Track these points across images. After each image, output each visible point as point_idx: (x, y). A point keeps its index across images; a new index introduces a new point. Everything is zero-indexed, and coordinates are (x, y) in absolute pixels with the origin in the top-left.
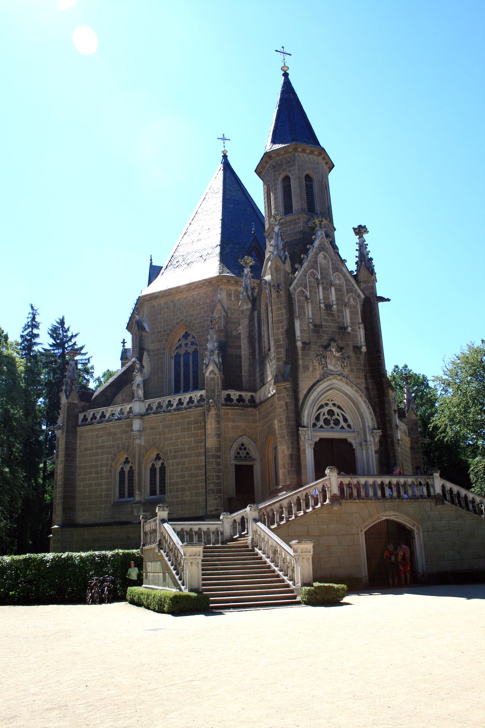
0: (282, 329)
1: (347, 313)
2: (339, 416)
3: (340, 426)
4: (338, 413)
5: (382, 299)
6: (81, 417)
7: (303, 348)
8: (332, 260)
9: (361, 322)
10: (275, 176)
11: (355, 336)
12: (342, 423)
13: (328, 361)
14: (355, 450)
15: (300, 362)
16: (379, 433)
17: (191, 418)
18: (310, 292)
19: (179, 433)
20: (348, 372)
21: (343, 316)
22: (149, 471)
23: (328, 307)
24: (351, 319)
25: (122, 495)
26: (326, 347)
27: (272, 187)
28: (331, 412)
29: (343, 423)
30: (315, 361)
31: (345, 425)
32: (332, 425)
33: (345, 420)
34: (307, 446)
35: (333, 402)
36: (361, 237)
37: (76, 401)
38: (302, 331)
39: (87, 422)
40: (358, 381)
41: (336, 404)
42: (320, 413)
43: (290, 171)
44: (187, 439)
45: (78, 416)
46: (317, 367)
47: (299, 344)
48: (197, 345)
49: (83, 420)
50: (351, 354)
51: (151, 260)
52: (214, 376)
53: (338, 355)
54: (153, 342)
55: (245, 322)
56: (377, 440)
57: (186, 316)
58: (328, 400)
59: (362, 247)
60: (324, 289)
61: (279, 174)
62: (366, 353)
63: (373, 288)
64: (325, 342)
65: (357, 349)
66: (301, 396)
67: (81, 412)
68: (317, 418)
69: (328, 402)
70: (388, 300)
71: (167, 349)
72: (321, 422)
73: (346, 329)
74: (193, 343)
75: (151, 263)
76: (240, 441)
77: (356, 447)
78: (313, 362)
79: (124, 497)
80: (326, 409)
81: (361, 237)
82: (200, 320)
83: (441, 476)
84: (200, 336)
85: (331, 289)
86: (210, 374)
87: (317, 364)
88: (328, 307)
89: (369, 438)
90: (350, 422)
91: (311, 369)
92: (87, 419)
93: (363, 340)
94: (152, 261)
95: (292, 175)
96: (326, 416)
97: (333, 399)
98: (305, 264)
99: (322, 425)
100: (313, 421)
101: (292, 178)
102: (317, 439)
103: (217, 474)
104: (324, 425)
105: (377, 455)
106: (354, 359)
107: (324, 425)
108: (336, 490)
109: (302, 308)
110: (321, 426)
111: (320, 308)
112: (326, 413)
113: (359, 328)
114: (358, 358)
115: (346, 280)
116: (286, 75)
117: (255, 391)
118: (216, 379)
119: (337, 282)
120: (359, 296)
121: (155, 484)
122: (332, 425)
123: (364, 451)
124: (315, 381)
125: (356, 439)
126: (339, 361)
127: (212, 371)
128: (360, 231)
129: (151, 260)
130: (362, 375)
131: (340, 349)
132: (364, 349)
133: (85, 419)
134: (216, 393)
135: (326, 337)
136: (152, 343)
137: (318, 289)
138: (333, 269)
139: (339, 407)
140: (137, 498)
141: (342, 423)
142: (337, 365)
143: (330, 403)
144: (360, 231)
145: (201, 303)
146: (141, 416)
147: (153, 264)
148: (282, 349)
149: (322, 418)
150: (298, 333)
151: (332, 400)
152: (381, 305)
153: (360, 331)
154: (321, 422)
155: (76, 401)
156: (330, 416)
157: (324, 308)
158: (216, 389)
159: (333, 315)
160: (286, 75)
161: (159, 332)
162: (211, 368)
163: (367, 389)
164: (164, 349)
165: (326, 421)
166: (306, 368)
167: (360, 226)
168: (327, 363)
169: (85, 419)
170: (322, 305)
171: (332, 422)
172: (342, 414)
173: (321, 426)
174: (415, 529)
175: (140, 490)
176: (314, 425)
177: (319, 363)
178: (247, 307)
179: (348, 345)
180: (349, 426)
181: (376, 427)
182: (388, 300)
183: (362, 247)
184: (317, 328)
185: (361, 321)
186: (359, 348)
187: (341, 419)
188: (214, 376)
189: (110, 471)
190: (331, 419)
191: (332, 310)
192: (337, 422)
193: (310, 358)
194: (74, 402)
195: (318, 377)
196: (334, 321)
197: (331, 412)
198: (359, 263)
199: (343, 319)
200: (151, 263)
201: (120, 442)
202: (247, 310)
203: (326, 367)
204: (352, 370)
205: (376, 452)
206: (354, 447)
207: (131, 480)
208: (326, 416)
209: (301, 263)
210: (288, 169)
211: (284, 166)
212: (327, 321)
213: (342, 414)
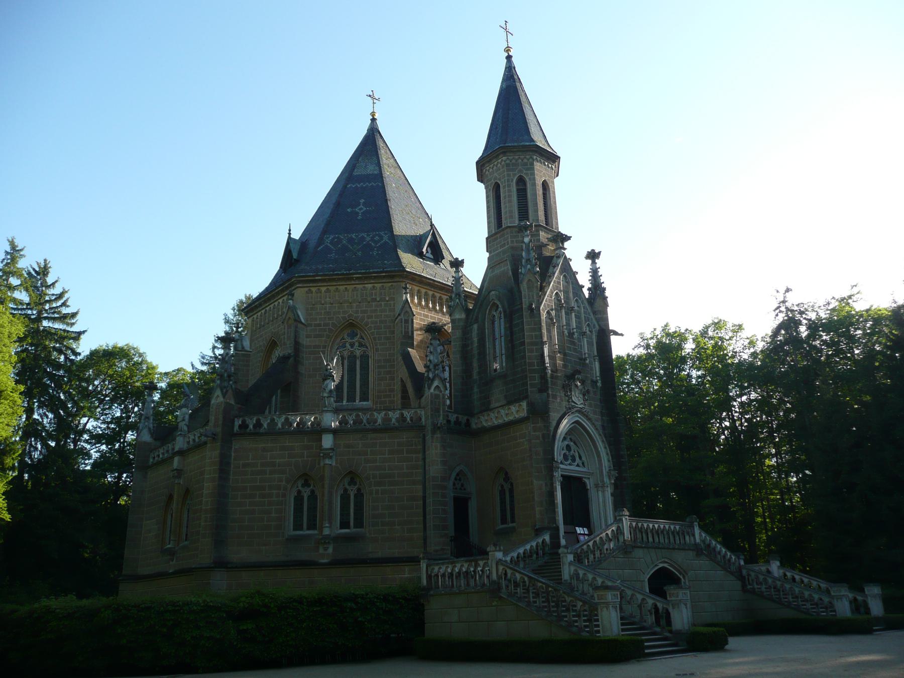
0: (536, 352)
3: (576, 464)
5: (616, 333)
6: (238, 422)
8: (572, 284)
9: (596, 354)
10: (509, 175)
11: (592, 369)
13: (573, 393)
14: (589, 493)
17: (403, 438)
19: (385, 455)
21: (581, 345)
22: (339, 498)
23: (571, 334)
24: (588, 351)
25: (298, 526)
27: (504, 187)
32: (569, 461)
33: (580, 458)
34: (557, 483)
36: (594, 263)
37: (232, 402)
39: (248, 430)
40: (596, 416)
43: (527, 174)
44: (396, 464)
45: (233, 422)
46: (564, 398)
48: (367, 347)
49: (240, 426)
50: (590, 389)
51: (290, 230)
52: (438, 393)
54: (307, 337)
55: (457, 333)
56: (613, 481)
57: (357, 312)
59: (595, 274)
60: (567, 314)
61: (514, 175)
62: (601, 387)
63: (606, 320)
65: (594, 383)
66: (552, 429)
67: (238, 416)
70: (622, 335)
71: (328, 348)
73: (585, 359)
74: (361, 345)
75: (290, 234)
76: (457, 470)
77: (591, 488)
78: (560, 392)
79: (301, 529)
80: (566, 443)
81: (594, 263)
82: (376, 320)
83: (700, 527)
84: (375, 339)
85: (571, 314)
86: (434, 390)
87: (563, 395)
89: (606, 480)
92: (247, 426)
93: (598, 374)
94: (291, 232)
95: (530, 179)
96: (565, 451)
101: (529, 183)
103: (443, 507)
104: (563, 461)
105: (613, 498)
106: (592, 394)
107: (563, 461)
111: (563, 334)
112: (565, 448)
113: (594, 360)
116: (509, 58)
117: (472, 415)
118: (441, 396)
121: (349, 514)
122: (569, 461)
123: (600, 493)
124: (562, 413)
125: (591, 479)
127: (437, 387)
128: (593, 256)
129: (290, 230)
132: (599, 384)
133: (244, 426)
134: (441, 413)
136: (307, 337)
137: (561, 313)
138: (573, 293)
139: (575, 443)
140: (326, 532)
142: (579, 398)
143: (569, 439)
144: (593, 256)
145: (378, 299)
146: (334, 432)
147: (292, 236)
148: (537, 375)
152: (613, 338)
153: (595, 364)
155: (232, 402)
157: (567, 334)
158: (441, 408)
159: (573, 343)
160: (509, 58)
161: (319, 325)
163: (603, 426)
164: (325, 347)
167: (593, 250)
168: (571, 394)
169: (244, 426)
170: (566, 332)
171: (570, 458)
174: (681, 577)
175: (330, 523)
177: (565, 394)
178: (460, 317)
180: (583, 464)
181: (612, 468)
182: (622, 335)
183: (595, 274)
185: (596, 354)
186: (596, 382)
187: (577, 455)
188: (438, 393)
189: (284, 496)
191: (573, 338)
192: (574, 460)
194: (231, 402)
196: (575, 350)
198: (593, 290)
199: (582, 349)
200: (290, 234)
201: (300, 460)
202: (460, 320)
203: (571, 397)
204: (590, 405)
205: (612, 495)
206: (589, 488)
207: (313, 509)
210: (524, 171)
211: (520, 167)
212: (570, 349)
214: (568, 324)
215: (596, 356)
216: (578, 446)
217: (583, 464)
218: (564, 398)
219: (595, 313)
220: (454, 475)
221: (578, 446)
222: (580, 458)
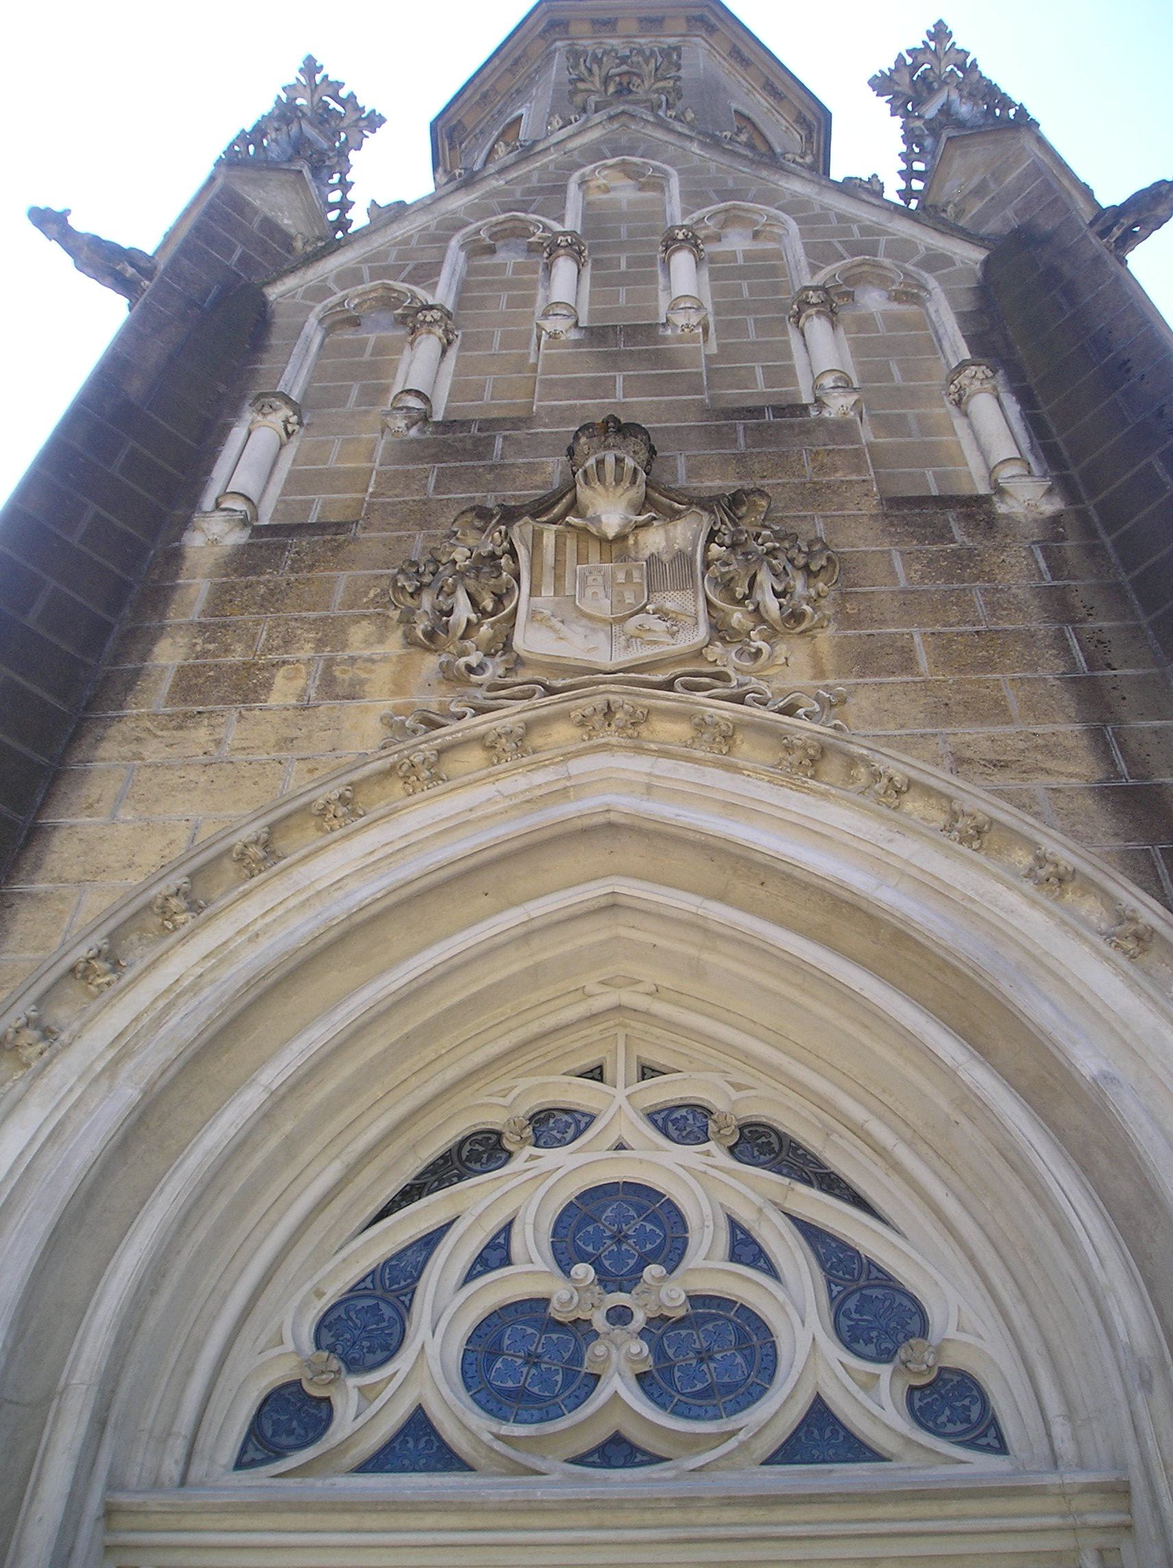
2: (771, 1270)
4: (746, 1217)
20: (820, 673)
29: (833, 1351)
30: (358, 634)
35: (662, 1092)
41: (718, 1103)
42: (430, 1241)
58: (596, 1073)
69: (582, 1095)
85: (666, 264)
97: (657, 1058)
99: (437, 1413)
110: (419, 1423)
126: (686, 581)
151: (647, 1072)
156: (583, 1271)
172: (811, 1233)
173: (419, 1423)
190: (620, 1316)
193: (313, 615)
213: (811, 1233)
215: (963, 365)
216: (831, 1183)
218: (383, 673)
221: (831, 1183)
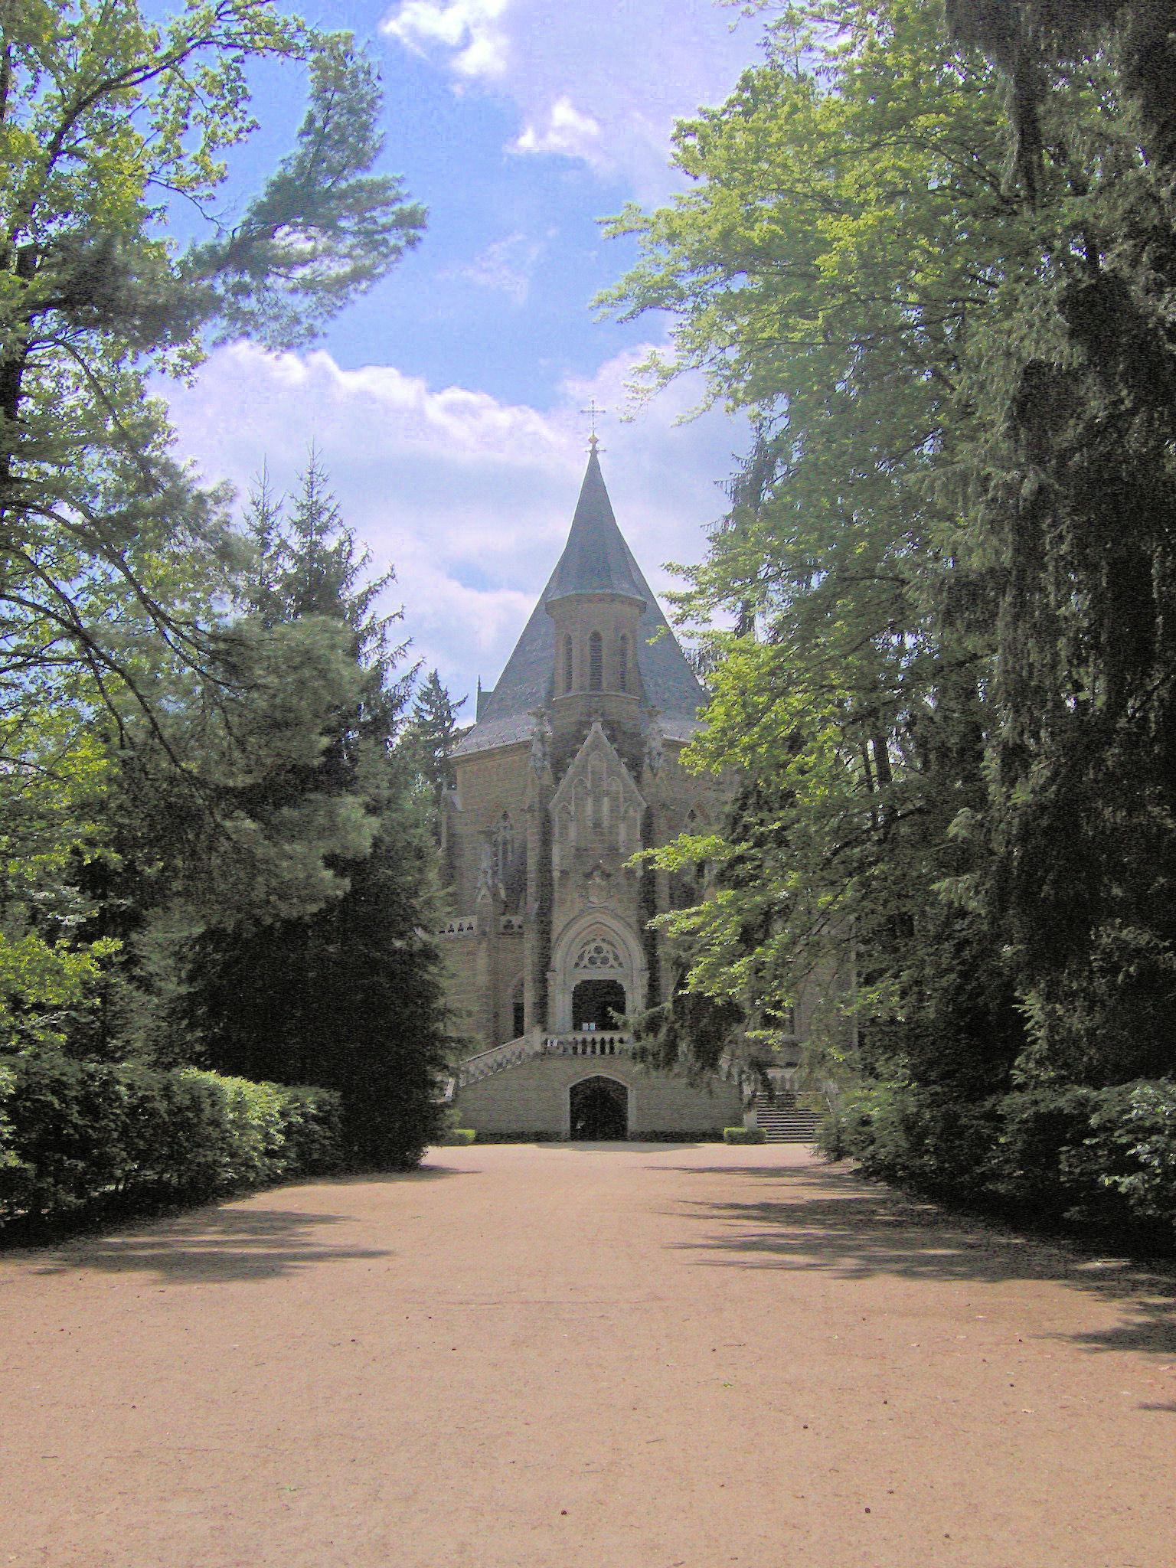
1: (622, 829)
7: (560, 879)
12: (612, 961)
15: (556, 895)
16: (647, 974)
18: (577, 806)
23: (597, 825)
26: (588, 876)
28: (598, 950)
31: (615, 964)
33: (616, 958)
38: (562, 858)
47: (556, 874)
50: (623, 881)
53: (604, 883)
64: (588, 869)
66: (554, 936)
68: (581, 957)
72: (586, 961)
80: (593, 946)
88: (597, 825)
90: (621, 959)
91: (569, 904)
96: (593, 954)
98: (571, 770)
100: (576, 960)
102: (578, 982)
108: (538, 1048)
109: (564, 827)
114: (631, 885)
115: (625, 785)
119: (614, 788)
120: (639, 805)
130: (634, 906)
131: (607, 876)
135: (591, 863)
139: (610, 943)
141: (612, 961)
149: (587, 957)
150: (556, 859)
154: (586, 961)
159: (602, 834)
162: (483, 892)
165: (592, 961)
166: (563, 902)
171: (599, 961)
176: (577, 965)
179: (618, 869)
180: (620, 964)
184: (580, 853)
185: (638, 836)
187: (611, 956)
192: (605, 961)
195: (576, 912)
196: (602, 841)
197: (598, 950)
204: (620, 901)
208: (593, 954)
209: (564, 771)
214: (597, 810)
217: (620, 964)
219: (641, 790)
220: (515, 981)
222: (616, 958)
